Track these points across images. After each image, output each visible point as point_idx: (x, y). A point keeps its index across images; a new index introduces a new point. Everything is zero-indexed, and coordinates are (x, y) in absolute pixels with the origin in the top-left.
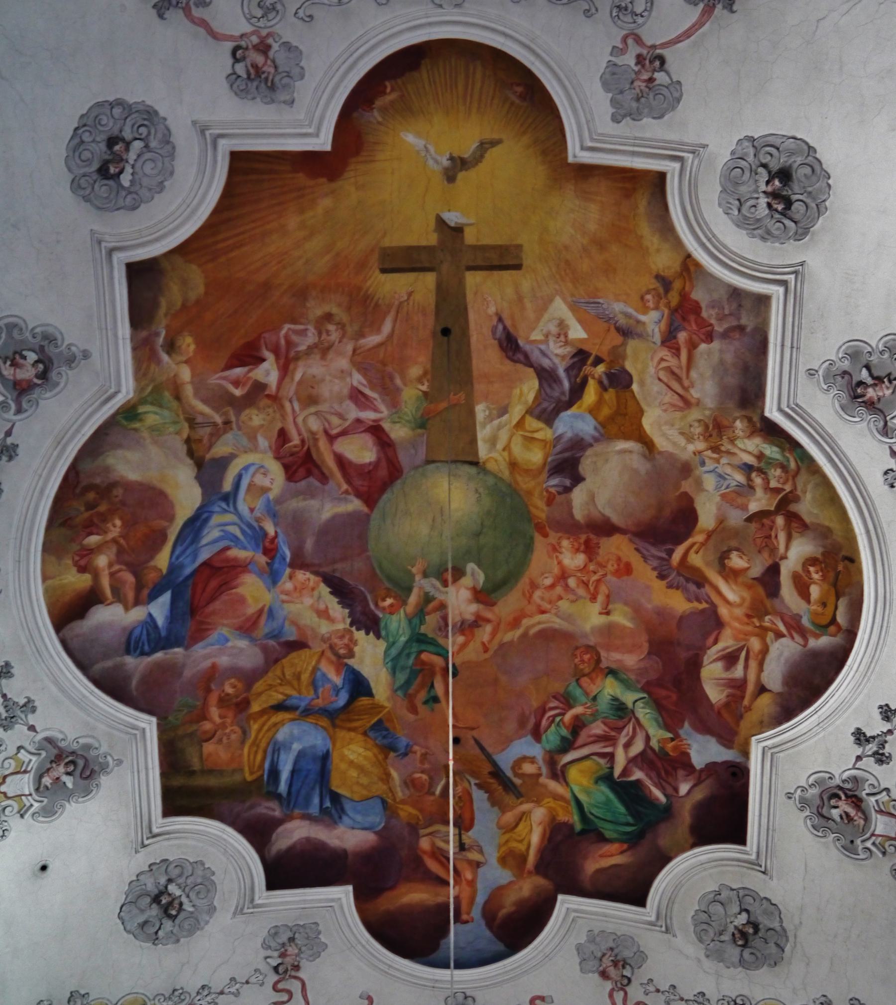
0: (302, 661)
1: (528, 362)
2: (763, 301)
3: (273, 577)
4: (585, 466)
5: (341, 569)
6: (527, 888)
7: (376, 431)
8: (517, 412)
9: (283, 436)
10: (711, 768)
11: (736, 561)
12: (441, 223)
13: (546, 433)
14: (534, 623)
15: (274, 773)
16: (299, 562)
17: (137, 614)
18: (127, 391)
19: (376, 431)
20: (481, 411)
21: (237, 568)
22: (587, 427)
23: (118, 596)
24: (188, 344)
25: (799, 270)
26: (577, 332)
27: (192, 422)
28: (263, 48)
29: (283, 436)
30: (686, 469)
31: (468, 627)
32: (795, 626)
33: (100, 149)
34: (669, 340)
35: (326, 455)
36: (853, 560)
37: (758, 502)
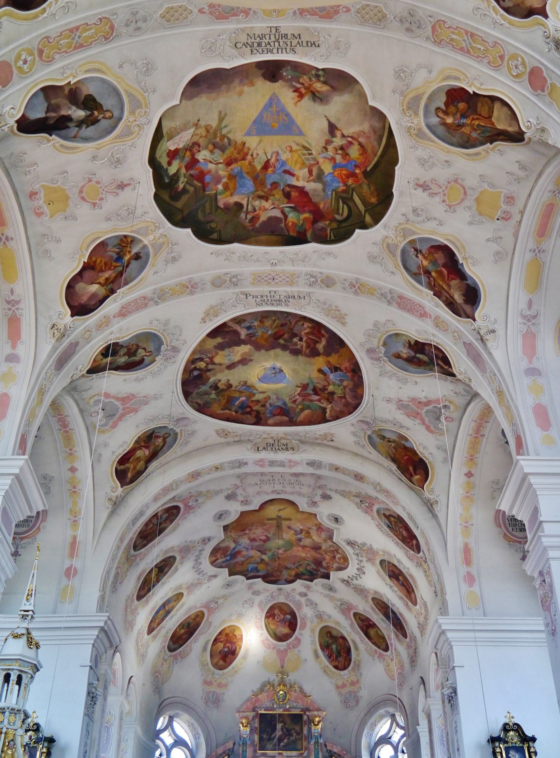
0: (253, 559)
1: (292, 529)
2: (333, 530)
3: (248, 551)
4: (303, 540)
5: (259, 549)
6: (292, 578)
7: (266, 536)
8: (290, 534)
9: (249, 537)
10: (324, 572)
11: (328, 554)
12: (277, 516)
13: (295, 536)
14: (294, 554)
15: (248, 570)
16: (252, 549)
17: (224, 559)
18: (223, 537)
19: (266, 536)
20: (284, 534)
21: (242, 551)
22: (303, 537)
23: (221, 558)
24: (233, 531)
25: (339, 529)
26: (301, 527)
27: (234, 538)
28: (247, 501)
29: (249, 537)
30: (320, 543)
31: (282, 554)
32: (338, 563)
33: (218, 516)
34: (317, 530)
35: (257, 539)
36: (348, 559)
37: (332, 549)
